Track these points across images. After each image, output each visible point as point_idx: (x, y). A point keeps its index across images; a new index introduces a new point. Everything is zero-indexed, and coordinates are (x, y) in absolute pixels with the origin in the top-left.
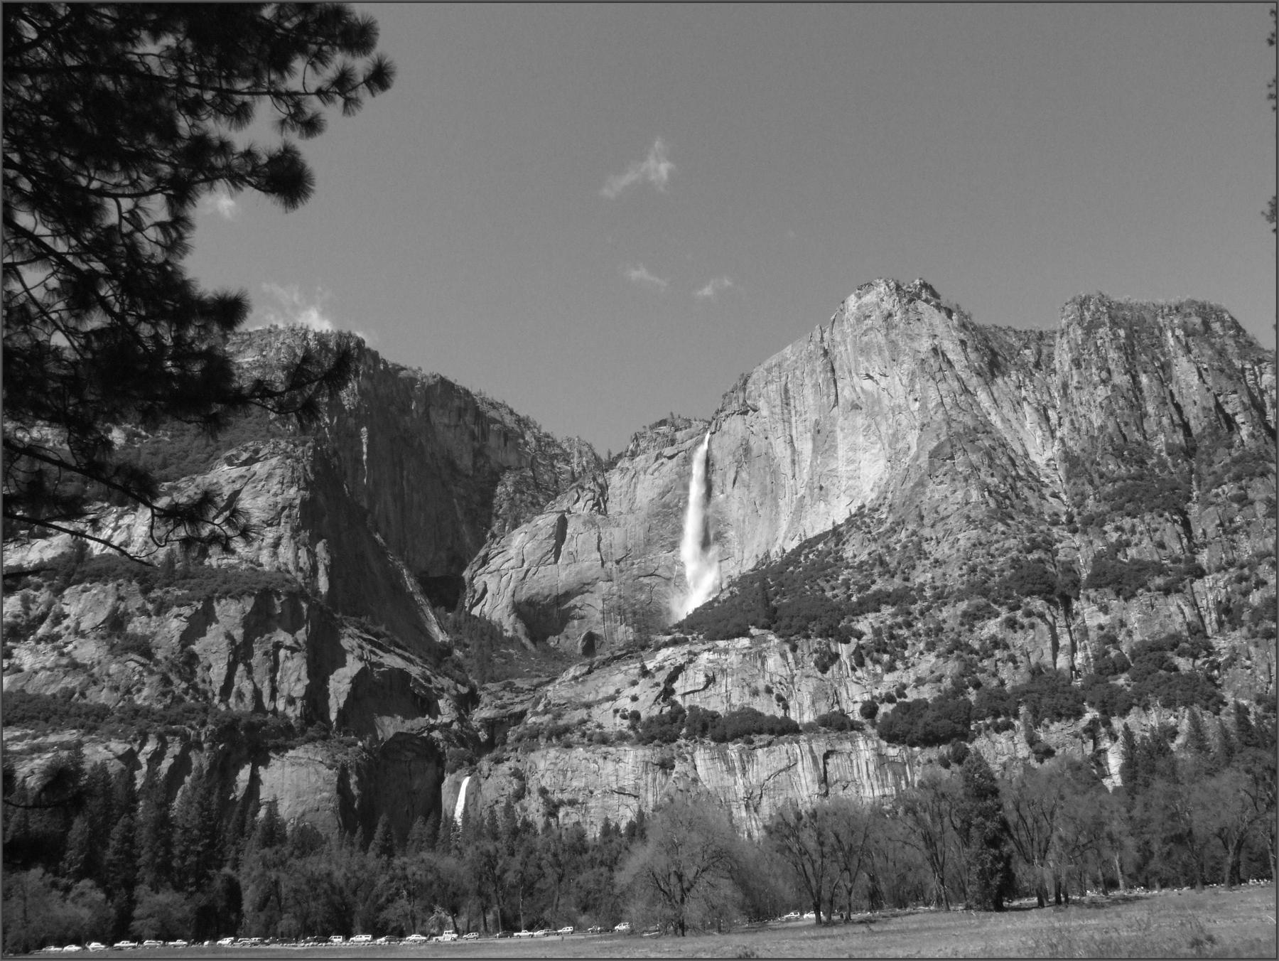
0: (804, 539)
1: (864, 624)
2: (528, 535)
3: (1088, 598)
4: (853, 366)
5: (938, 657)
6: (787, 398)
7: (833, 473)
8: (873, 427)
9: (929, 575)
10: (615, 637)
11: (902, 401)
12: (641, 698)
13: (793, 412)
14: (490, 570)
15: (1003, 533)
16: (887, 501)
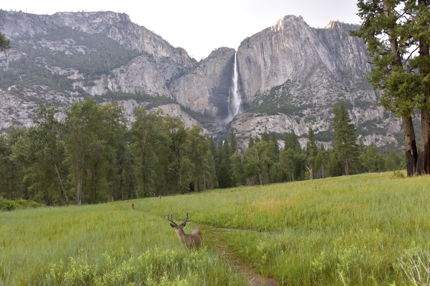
0: (273, 87)
1: (305, 112)
2: (185, 80)
3: (355, 109)
4: (283, 40)
5: (324, 121)
6: (263, 46)
7: (278, 69)
8: (289, 58)
9: (316, 101)
10: (212, 110)
11: (298, 52)
12: (261, 129)
13: (264, 50)
14: (175, 90)
15: (333, 91)
16: (298, 79)
